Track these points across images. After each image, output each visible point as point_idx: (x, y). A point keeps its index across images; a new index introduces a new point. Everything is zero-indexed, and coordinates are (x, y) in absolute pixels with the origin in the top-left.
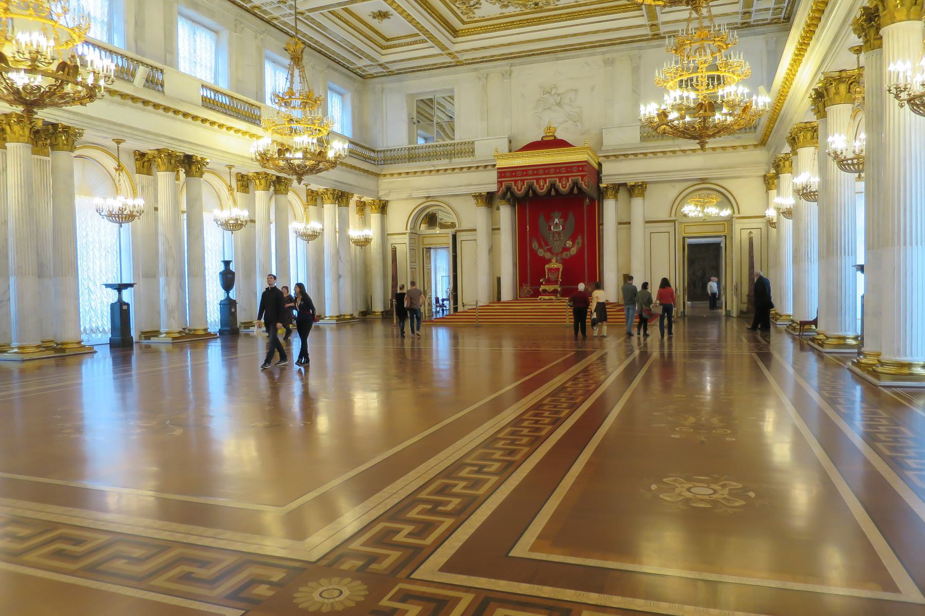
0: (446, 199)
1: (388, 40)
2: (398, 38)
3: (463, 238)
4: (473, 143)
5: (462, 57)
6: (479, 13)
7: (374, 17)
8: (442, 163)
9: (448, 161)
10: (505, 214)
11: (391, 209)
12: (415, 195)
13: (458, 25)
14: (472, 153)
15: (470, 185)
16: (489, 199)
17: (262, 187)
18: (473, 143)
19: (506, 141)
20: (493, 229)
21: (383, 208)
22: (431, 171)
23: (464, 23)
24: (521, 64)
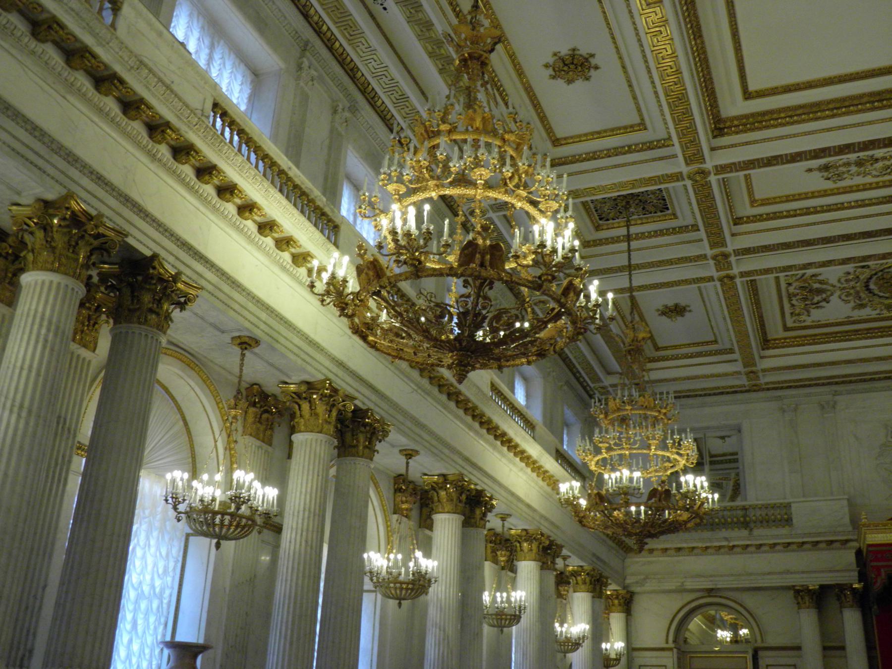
0: (737, 595)
1: (657, 349)
2: (675, 347)
3: (770, 661)
4: (788, 506)
5: (764, 380)
6: (817, 315)
7: (663, 313)
8: (739, 537)
9: (745, 533)
10: (852, 624)
11: (641, 605)
12: (689, 585)
13: (775, 331)
14: (788, 521)
15: (788, 572)
16: (820, 598)
17: (533, 554)
18: (788, 506)
19: (845, 503)
20: (825, 648)
21: (627, 603)
22: (720, 547)
23: (786, 329)
24: (849, 393)
